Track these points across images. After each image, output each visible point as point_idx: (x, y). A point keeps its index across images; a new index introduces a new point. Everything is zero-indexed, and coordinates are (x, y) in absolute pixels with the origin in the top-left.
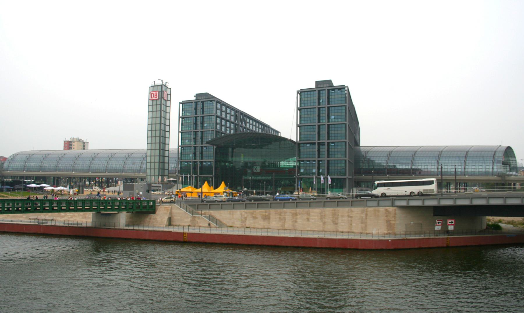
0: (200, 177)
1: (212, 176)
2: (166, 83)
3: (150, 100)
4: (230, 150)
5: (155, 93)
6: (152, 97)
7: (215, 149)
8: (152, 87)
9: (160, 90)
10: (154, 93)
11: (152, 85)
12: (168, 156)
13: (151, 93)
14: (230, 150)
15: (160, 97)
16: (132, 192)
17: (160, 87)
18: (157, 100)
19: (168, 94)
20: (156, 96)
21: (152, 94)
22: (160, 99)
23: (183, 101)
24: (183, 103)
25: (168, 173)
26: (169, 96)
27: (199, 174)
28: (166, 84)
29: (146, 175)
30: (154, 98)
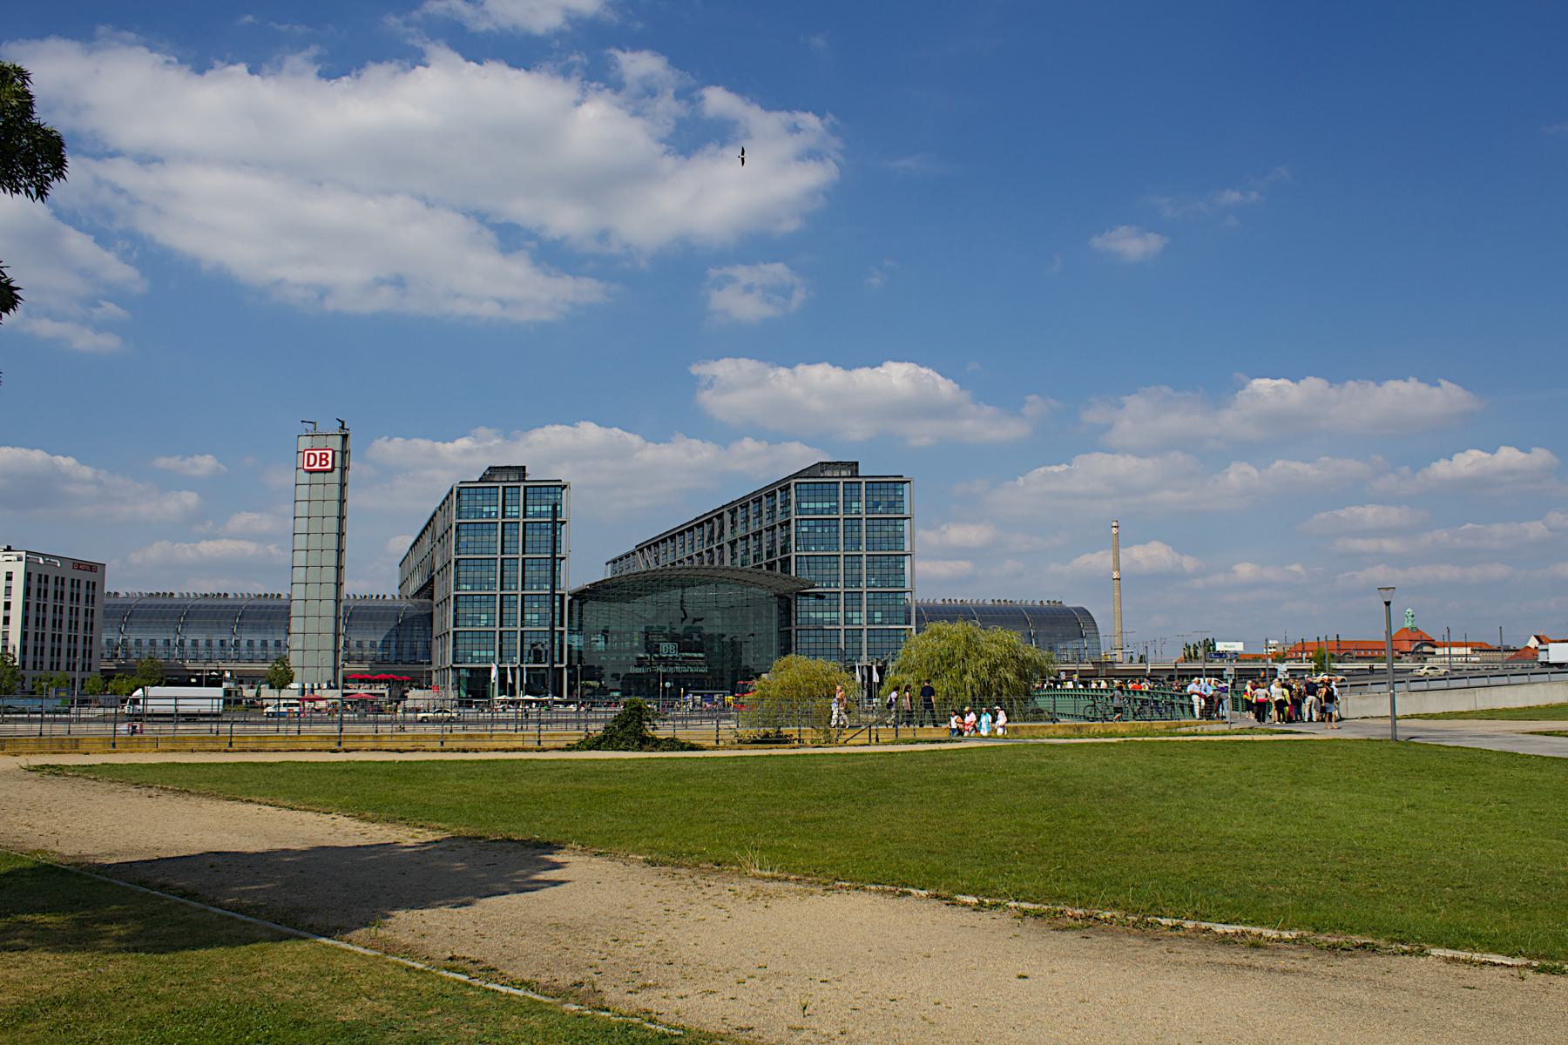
5: (321, 454)
9: (338, 447)
10: (317, 453)
13: (307, 452)
15: (338, 463)
17: (339, 439)
18: (325, 471)
20: (324, 463)
21: (309, 455)
22: (337, 471)
23: (461, 482)
30: (317, 467)
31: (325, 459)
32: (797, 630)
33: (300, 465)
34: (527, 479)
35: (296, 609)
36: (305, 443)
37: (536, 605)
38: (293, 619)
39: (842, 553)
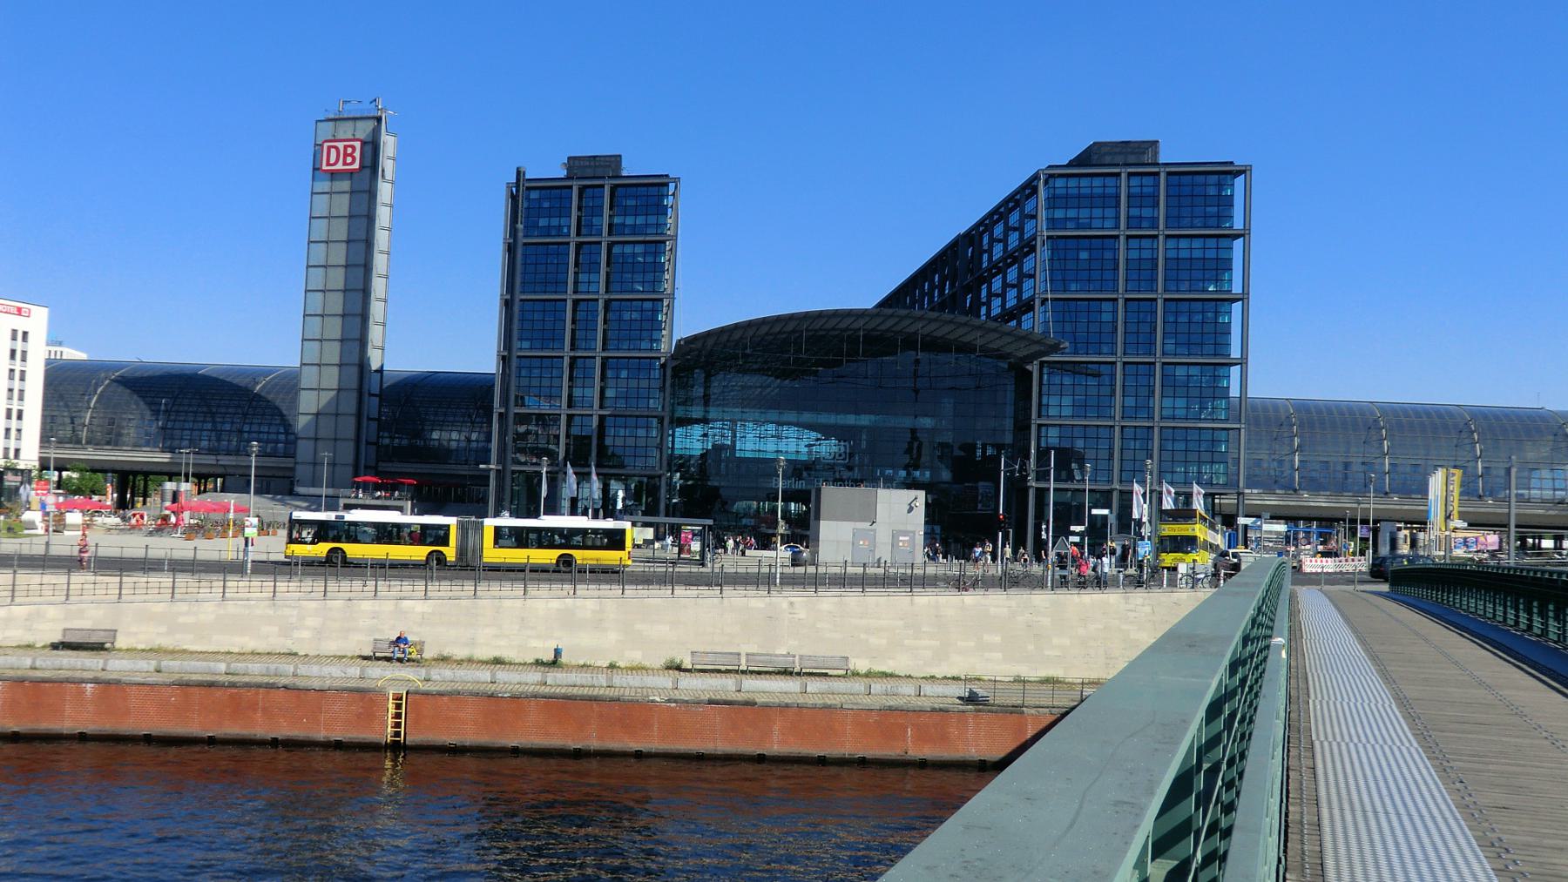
3: (317, 172)
4: (699, 375)
5: (346, 147)
6: (332, 160)
7: (673, 368)
8: (331, 124)
10: (341, 145)
11: (332, 116)
13: (326, 145)
14: (699, 375)
15: (368, 162)
16: (866, 525)
18: (352, 172)
20: (349, 160)
21: (329, 148)
22: (367, 172)
25: (378, 461)
29: (296, 463)
30: (340, 166)
31: (351, 155)
33: (317, 166)
34: (624, 173)
35: (309, 378)
36: (326, 130)
37: (624, 374)
38: (302, 392)
39: (1121, 295)
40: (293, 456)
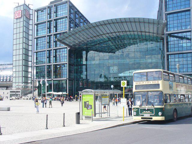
0: (54, 80)
1: (65, 79)
2: (29, 4)
4: (84, 52)
9: (22, 10)
10: (18, 12)
12: (31, 66)
14: (84, 52)
18: (20, 18)
19: (30, 15)
20: (19, 15)
24: (37, 11)
26: (31, 16)
27: (53, 78)
28: (29, 5)
30: (18, 17)
32: (168, 55)
40: (12, 81)
